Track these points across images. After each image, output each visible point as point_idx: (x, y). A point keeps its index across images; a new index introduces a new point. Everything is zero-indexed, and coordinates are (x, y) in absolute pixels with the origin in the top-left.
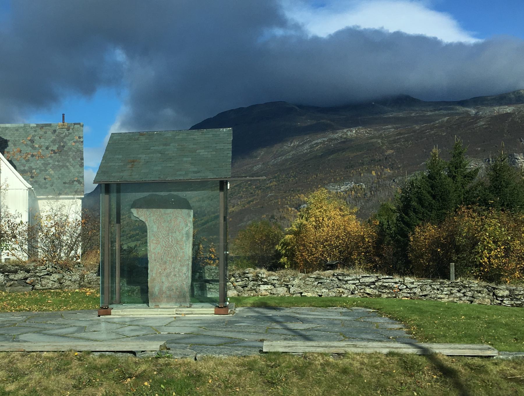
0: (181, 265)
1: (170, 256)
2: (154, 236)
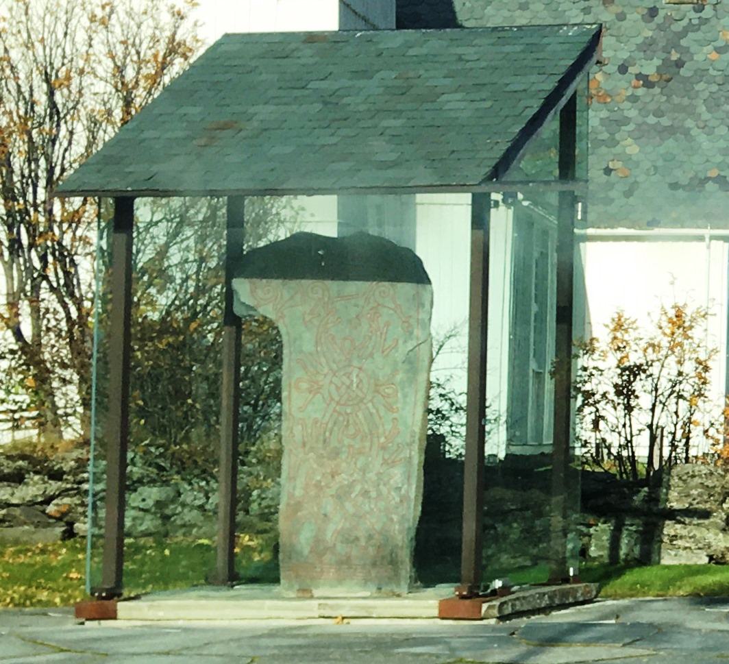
1: (352, 431)
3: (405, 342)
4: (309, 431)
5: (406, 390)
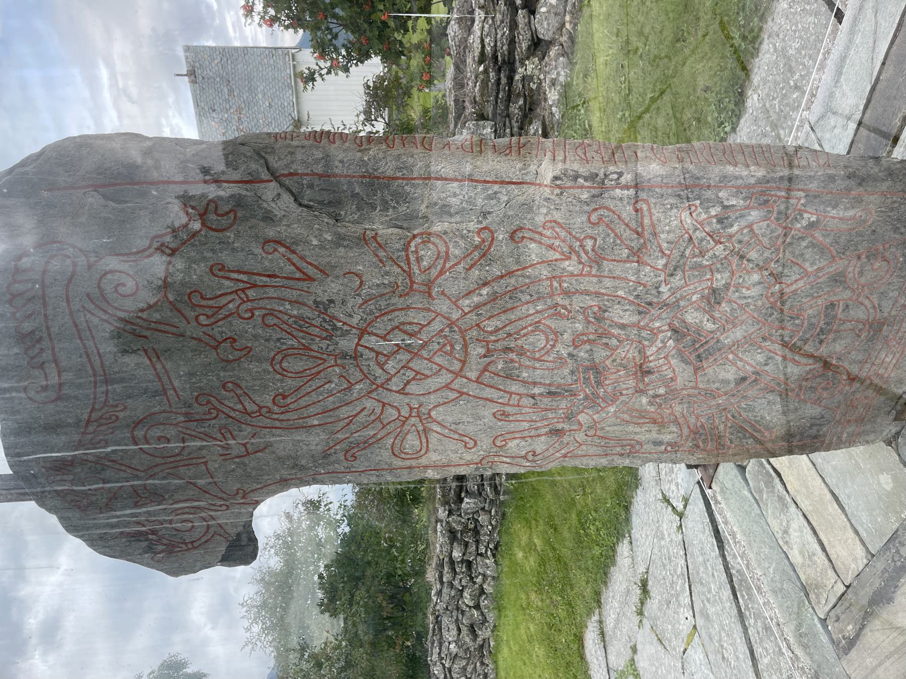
3: (268, 218)
4: (526, 425)
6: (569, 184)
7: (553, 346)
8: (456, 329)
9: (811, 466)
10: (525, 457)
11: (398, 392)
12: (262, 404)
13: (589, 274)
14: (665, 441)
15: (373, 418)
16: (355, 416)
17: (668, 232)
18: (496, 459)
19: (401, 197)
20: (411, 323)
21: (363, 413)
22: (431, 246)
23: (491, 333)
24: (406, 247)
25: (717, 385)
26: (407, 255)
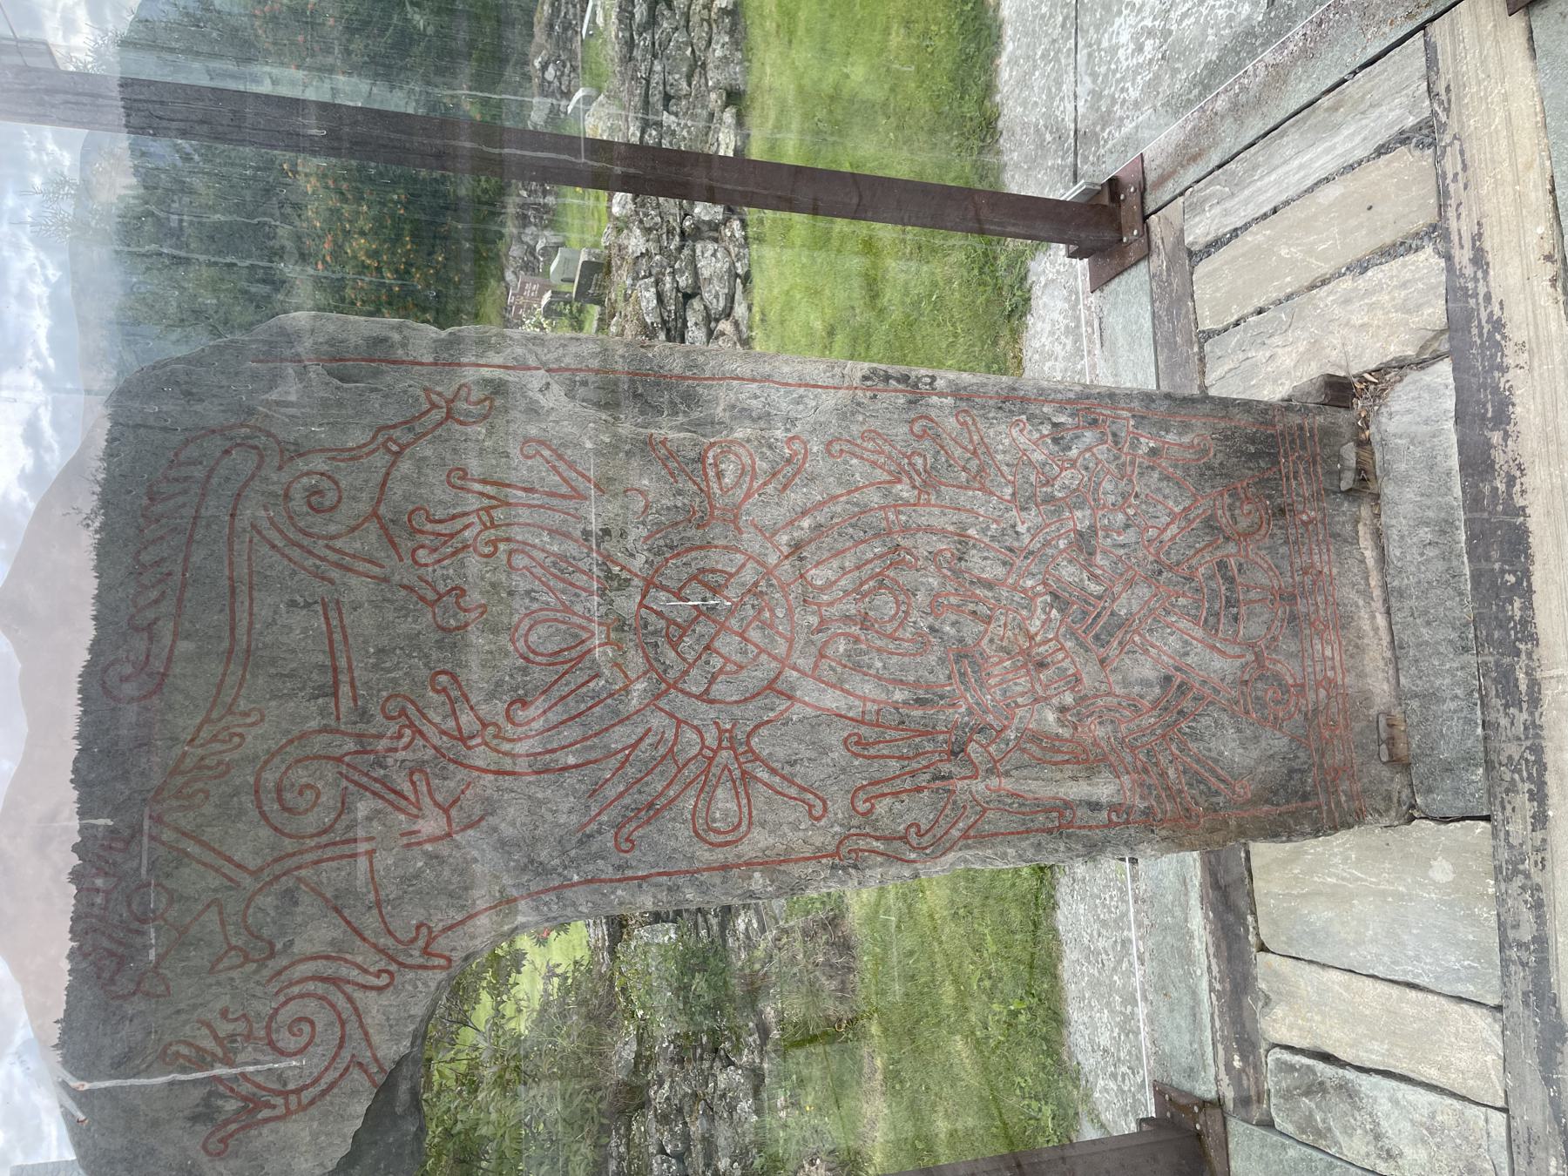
0: (979, 479)
2: (651, 810)
3: (533, 411)
5: (719, 412)
6: (881, 386)
7: (906, 613)
8: (774, 582)
9: (1347, 976)
10: (904, 838)
11: (697, 697)
12: (489, 718)
13: (928, 504)
14: (1104, 800)
15: (662, 750)
16: (634, 746)
17: (1004, 452)
18: (862, 844)
19: (690, 399)
20: (713, 571)
21: (648, 741)
22: (733, 458)
23: (822, 589)
24: (701, 459)
25: (1137, 689)
26: (704, 469)
